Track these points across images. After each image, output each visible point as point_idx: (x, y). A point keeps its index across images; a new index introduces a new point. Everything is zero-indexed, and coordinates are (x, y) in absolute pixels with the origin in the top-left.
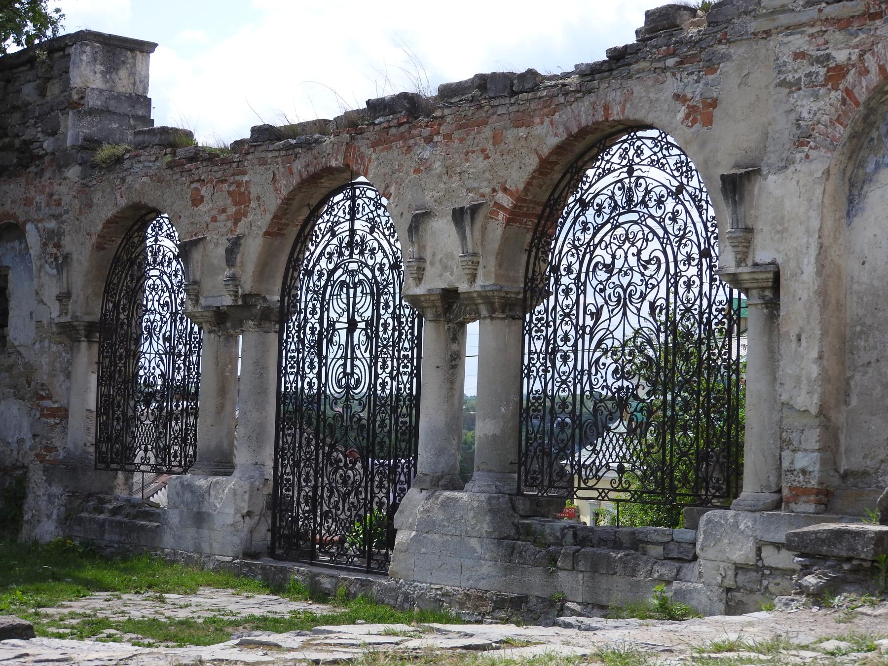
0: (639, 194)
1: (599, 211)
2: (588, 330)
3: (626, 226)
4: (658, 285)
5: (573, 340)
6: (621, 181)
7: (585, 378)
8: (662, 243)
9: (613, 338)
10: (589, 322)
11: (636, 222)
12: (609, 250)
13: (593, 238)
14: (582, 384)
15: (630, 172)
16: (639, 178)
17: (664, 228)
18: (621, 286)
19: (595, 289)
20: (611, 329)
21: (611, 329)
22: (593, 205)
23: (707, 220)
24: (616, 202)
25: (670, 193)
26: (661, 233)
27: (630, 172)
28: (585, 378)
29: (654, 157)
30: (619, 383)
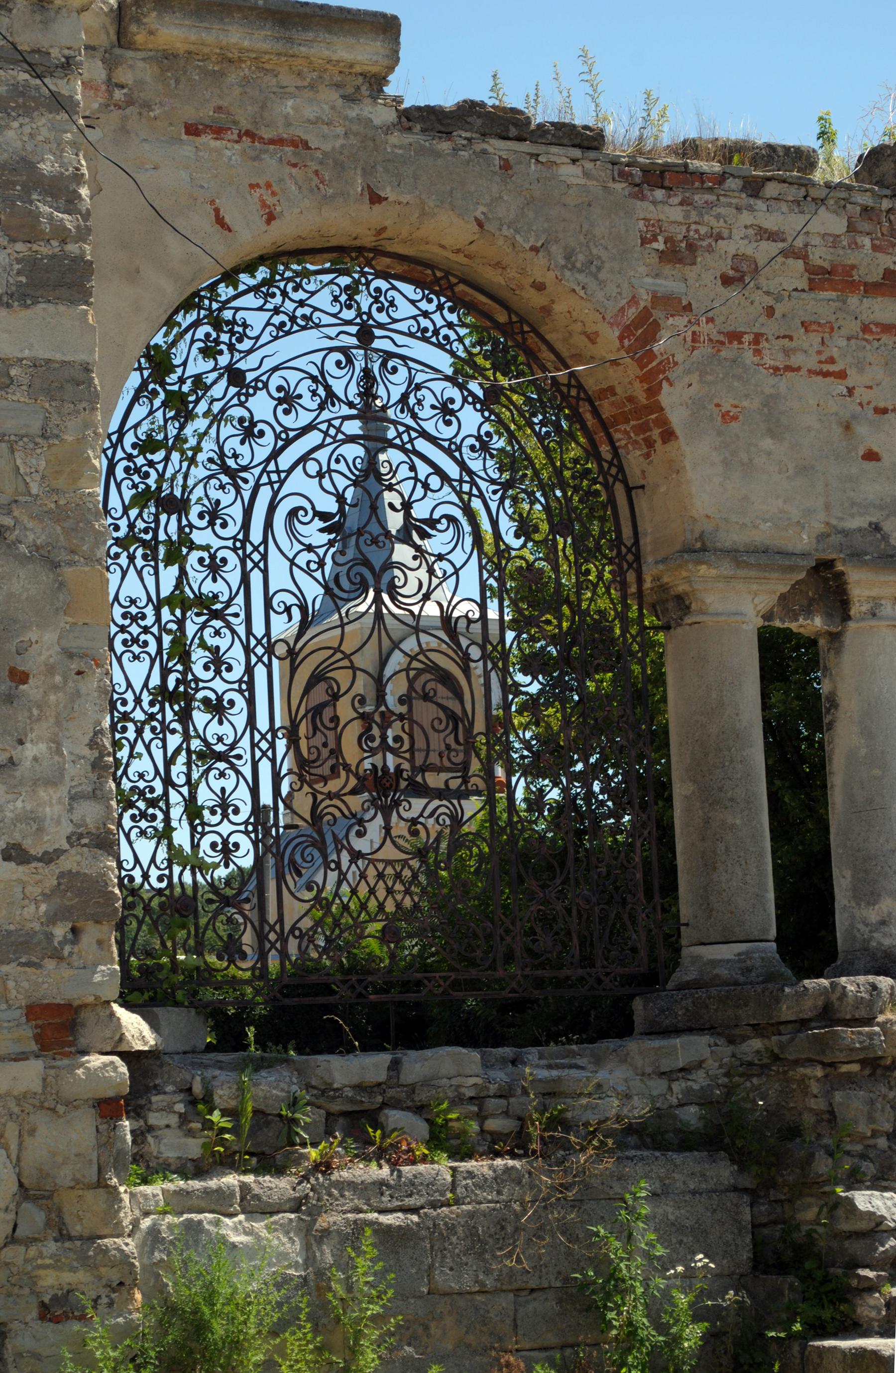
1: (288, 400)
2: (281, 649)
4: (456, 572)
6: (344, 350)
7: (281, 745)
8: (459, 494)
9: (354, 668)
12: (326, 482)
13: (275, 454)
14: (273, 761)
15: (365, 336)
16: (390, 355)
17: (462, 465)
18: (366, 563)
19: (292, 562)
20: (347, 648)
21: (347, 648)
22: (266, 385)
23: (563, 464)
24: (328, 388)
25: (469, 398)
26: (453, 471)
27: (365, 336)
29: (424, 323)
30: (378, 760)
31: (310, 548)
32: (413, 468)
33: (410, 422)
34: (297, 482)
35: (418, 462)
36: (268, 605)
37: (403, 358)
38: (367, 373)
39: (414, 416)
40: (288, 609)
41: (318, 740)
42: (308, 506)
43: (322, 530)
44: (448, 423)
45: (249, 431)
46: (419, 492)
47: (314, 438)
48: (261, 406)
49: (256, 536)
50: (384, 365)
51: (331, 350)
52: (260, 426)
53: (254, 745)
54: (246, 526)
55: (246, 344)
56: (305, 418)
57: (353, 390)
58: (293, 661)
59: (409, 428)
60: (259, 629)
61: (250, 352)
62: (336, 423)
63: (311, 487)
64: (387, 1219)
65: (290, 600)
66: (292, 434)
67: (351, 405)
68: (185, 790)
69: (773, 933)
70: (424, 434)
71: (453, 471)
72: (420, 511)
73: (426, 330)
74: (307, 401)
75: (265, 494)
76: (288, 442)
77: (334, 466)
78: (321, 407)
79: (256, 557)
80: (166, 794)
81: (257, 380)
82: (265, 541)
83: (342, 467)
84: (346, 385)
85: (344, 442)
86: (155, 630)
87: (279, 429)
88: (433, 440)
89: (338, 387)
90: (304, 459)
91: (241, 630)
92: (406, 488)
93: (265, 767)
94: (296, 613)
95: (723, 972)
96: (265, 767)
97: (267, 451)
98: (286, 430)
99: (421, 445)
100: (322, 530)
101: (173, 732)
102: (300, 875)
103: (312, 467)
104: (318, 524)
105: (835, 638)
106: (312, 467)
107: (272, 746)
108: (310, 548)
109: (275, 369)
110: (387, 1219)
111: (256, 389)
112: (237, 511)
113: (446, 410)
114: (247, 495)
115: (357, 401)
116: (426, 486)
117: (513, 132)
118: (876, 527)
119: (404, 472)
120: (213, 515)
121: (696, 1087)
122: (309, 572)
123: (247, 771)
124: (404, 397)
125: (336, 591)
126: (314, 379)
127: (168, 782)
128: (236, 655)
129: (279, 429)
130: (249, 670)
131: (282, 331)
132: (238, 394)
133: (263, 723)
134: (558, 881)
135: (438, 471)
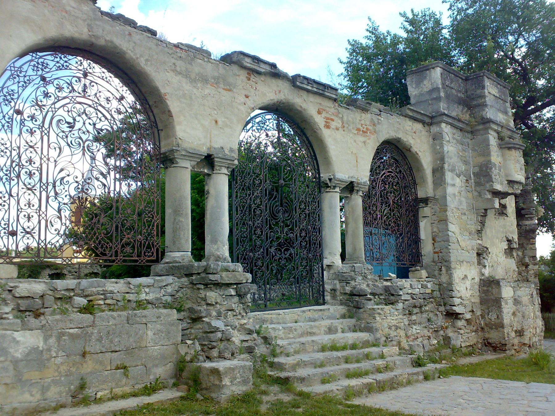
0: (91, 91)
3: (85, 106)
5: (37, 164)
6: (79, 78)
7: (50, 187)
8: (110, 123)
10: (54, 154)
11: (90, 106)
12: (70, 114)
13: (54, 103)
14: (47, 192)
15: (85, 75)
16: (92, 82)
18: (80, 138)
19: (57, 135)
22: (53, 83)
24: (72, 87)
26: (109, 117)
27: (85, 75)
28: (50, 187)
31: (63, 132)
32: (97, 114)
33: (97, 101)
34: (61, 112)
35: (98, 112)
36: (49, 146)
37: (97, 83)
38: (85, 85)
39: (98, 100)
40: (55, 148)
41: (62, 187)
42: (64, 120)
43: (67, 127)
44: (108, 103)
45: (46, 95)
46: (98, 121)
47: (67, 101)
48: (51, 89)
49: (46, 125)
50: (90, 84)
51: (74, 77)
52: (50, 94)
53: (41, 187)
54: (43, 122)
55: (47, 70)
56: (64, 95)
57: (80, 90)
58: (55, 164)
59: (96, 103)
60: (45, 153)
61: (48, 72)
62: (75, 98)
63: (65, 114)
64: (71, 331)
65: (56, 146)
66: (60, 98)
67: (79, 93)
68: (16, 198)
69: (190, 250)
70: (101, 105)
71: (109, 117)
72: (98, 126)
73: (103, 77)
74: (65, 89)
75: (50, 114)
76: (59, 100)
77: (73, 109)
78: (70, 92)
79: (46, 132)
80: (9, 199)
81: (50, 81)
82: (49, 128)
83: (75, 110)
84: (78, 87)
85: (76, 103)
86: (10, 149)
87: (56, 96)
88: (104, 107)
89: (76, 88)
90: (63, 106)
91: (39, 152)
92: (94, 119)
93: (44, 194)
94: (58, 150)
95: (177, 259)
96: (44, 194)
97: (52, 102)
98: (58, 97)
99: (100, 108)
100: (67, 127)
101: (13, 180)
102: (53, 226)
103: (66, 109)
104: (67, 125)
105: (209, 175)
106: (66, 109)
107: (47, 187)
108: (63, 132)
109: (55, 79)
110: (71, 331)
111: (50, 83)
112: (40, 118)
113: (108, 100)
114: (44, 114)
115: (81, 92)
116: (100, 120)
117: (132, 25)
118: (222, 148)
119: (94, 114)
120: (33, 117)
121: (168, 291)
122: (62, 138)
123: (38, 194)
124: (96, 94)
125: (71, 145)
126: (69, 84)
127: (10, 195)
128: (37, 160)
129: (56, 96)
130: (41, 165)
131: (59, 69)
132: (44, 84)
133: (44, 181)
134: (132, 233)
135: (104, 116)
